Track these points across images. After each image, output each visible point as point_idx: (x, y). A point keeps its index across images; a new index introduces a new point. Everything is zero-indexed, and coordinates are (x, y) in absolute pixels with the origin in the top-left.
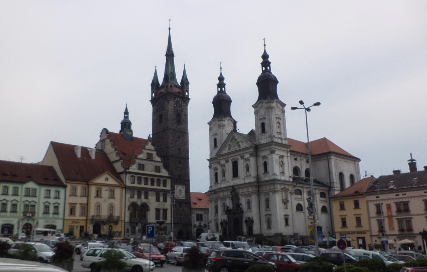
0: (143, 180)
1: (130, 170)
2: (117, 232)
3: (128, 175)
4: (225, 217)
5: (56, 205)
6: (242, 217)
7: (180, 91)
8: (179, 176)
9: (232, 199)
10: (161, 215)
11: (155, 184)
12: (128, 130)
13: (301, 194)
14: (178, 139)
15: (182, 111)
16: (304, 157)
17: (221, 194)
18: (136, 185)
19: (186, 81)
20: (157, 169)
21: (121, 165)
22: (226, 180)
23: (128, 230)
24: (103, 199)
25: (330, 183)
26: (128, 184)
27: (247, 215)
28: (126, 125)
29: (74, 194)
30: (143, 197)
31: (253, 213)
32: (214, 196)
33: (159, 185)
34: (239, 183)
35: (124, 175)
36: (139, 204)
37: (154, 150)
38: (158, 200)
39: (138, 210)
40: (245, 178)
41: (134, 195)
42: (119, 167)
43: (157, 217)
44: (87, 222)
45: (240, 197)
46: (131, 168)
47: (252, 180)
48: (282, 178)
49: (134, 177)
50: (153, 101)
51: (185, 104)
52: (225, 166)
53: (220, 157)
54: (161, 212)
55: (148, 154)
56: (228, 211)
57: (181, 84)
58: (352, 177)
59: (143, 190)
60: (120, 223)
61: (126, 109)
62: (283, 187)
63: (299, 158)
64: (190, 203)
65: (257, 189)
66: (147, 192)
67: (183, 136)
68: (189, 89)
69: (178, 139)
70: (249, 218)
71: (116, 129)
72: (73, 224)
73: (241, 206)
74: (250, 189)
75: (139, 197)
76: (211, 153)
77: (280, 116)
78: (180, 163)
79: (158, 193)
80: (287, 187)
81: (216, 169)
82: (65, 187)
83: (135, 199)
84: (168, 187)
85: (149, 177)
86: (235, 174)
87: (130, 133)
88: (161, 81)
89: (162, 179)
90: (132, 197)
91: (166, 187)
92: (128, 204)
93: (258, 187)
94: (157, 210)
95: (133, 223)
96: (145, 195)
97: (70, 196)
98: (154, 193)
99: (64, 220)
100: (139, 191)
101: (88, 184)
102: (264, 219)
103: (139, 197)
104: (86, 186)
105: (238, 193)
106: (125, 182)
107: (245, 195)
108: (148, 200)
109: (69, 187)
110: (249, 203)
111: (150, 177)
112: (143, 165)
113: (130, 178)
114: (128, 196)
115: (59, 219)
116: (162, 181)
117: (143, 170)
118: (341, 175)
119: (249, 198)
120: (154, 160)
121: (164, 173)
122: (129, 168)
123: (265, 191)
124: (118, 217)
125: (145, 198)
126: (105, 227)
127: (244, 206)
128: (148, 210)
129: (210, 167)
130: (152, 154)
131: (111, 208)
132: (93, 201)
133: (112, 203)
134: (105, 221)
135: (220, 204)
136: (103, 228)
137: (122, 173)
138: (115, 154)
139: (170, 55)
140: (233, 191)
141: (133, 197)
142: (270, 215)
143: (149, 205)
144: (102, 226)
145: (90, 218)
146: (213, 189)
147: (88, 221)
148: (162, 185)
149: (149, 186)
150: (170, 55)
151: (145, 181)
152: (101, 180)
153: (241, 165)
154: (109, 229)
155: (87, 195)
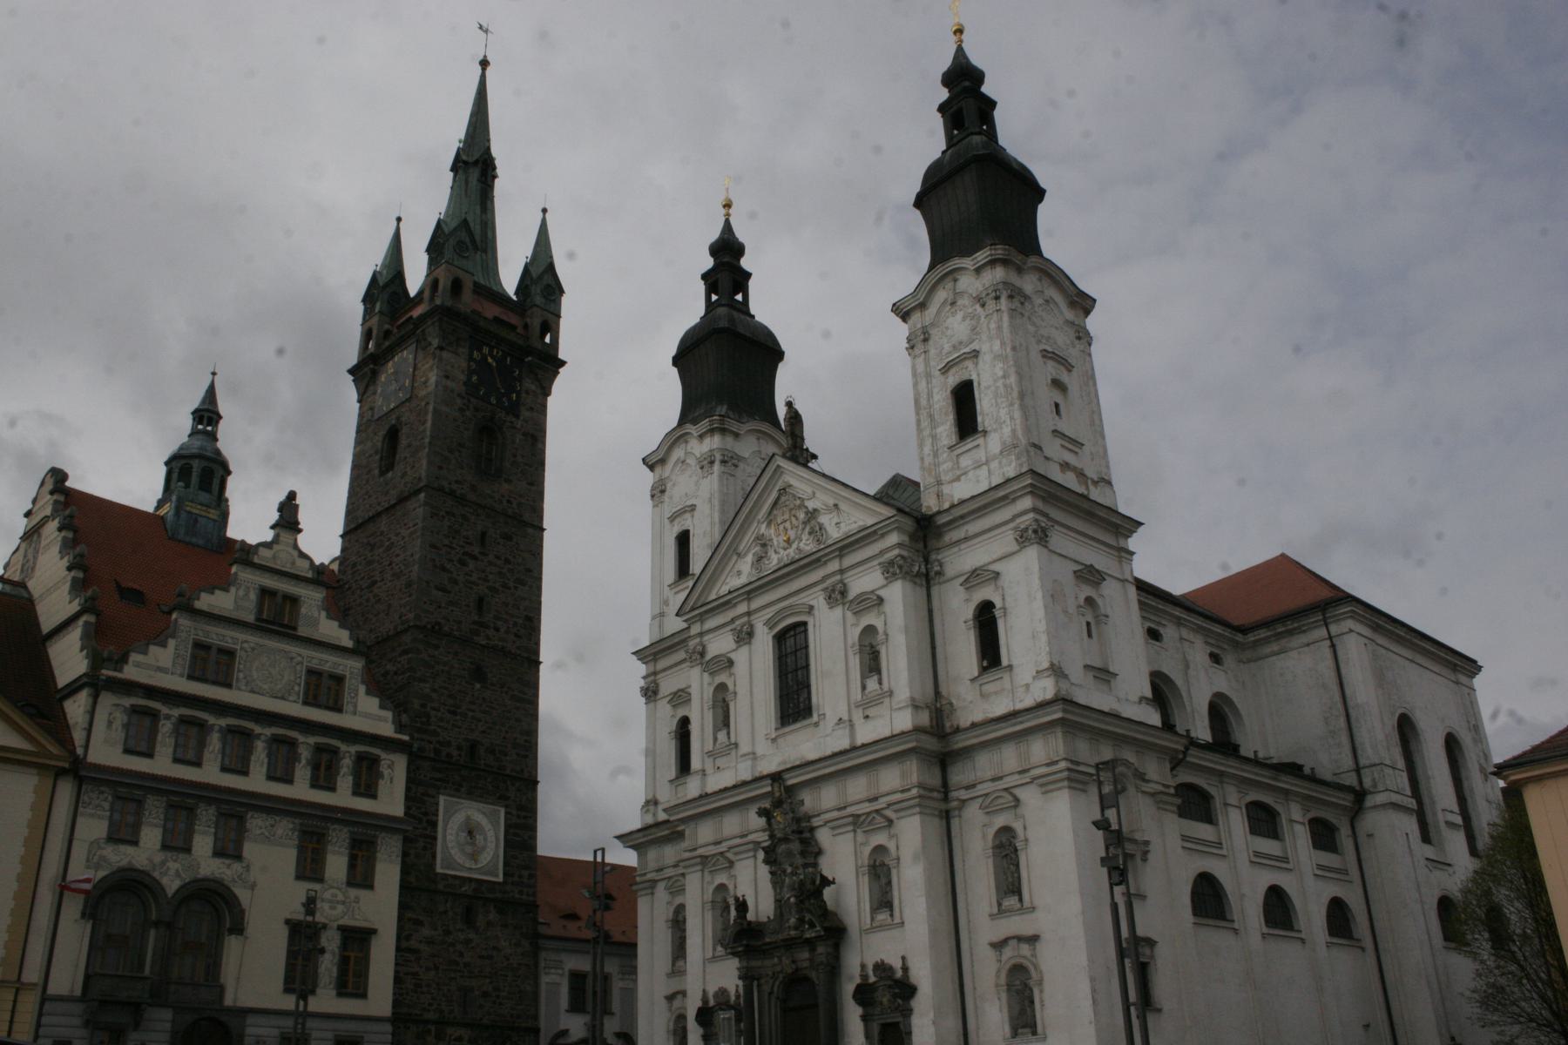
0: (214, 742)
1: (130, 672)
3: (107, 700)
4: (727, 976)
6: (834, 969)
7: (514, 319)
8: (473, 747)
10: (328, 966)
11: (302, 773)
12: (204, 497)
13: (1208, 817)
14: (476, 550)
15: (514, 409)
16: (1198, 630)
17: (704, 833)
18: (162, 764)
19: (547, 279)
20: (323, 688)
21: (79, 644)
22: (736, 745)
25: (1358, 770)
26: (105, 751)
27: (870, 949)
28: (199, 471)
30: (203, 844)
31: (906, 941)
32: (670, 853)
33: (324, 777)
34: (812, 756)
35: (83, 697)
36: (171, 885)
38: (310, 867)
39: (157, 924)
40: (857, 716)
41: (136, 827)
42: (68, 659)
43: (299, 978)
45: (823, 837)
46: (134, 657)
47: (904, 721)
48: (1099, 699)
49: (154, 715)
50: (365, 372)
51: (529, 384)
52: (731, 663)
53: (701, 618)
54: (331, 942)
55: (265, 593)
56: (743, 937)
57: (516, 293)
58: (1452, 745)
59: (210, 801)
61: (211, 393)
62: (1107, 754)
63: (1169, 632)
64: (532, 907)
65: (935, 781)
67: (507, 537)
68: (559, 316)
69: (476, 550)
70: (881, 967)
71: (132, 479)
73: (828, 893)
74: (890, 779)
75: (176, 843)
77: (1061, 339)
78: (479, 674)
79: (313, 830)
80: (1129, 755)
81: (680, 697)
83: (147, 850)
84: (391, 800)
86: (794, 702)
87: (213, 514)
88: (416, 276)
89: (349, 750)
90: (123, 834)
91: (374, 797)
93: (944, 760)
94: (303, 935)
100: (183, 801)
102: (986, 972)
103: (176, 843)
105: (809, 818)
106: (78, 736)
107: (857, 821)
108: (237, 866)
110: (880, 871)
112: (230, 654)
113: (120, 718)
114: (93, 828)
116: (347, 763)
118: (1406, 728)
119: (880, 839)
120: (303, 631)
121: (368, 713)
122: (124, 659)
123: (982, 789)
125: (219, 853)
127: (848, 891)
128: (238, 929)
130: (294, 600)
135: (696, 892)
137: (73, 688)
138: (67, 586)
139: (475, 167)
140: (778, 804)
141: (135, 843)
142: (1033, 939)
143: (242, 894)
148: (345, 782)
149: (256, 781)
150: (475, 167)
153: (831, 638)
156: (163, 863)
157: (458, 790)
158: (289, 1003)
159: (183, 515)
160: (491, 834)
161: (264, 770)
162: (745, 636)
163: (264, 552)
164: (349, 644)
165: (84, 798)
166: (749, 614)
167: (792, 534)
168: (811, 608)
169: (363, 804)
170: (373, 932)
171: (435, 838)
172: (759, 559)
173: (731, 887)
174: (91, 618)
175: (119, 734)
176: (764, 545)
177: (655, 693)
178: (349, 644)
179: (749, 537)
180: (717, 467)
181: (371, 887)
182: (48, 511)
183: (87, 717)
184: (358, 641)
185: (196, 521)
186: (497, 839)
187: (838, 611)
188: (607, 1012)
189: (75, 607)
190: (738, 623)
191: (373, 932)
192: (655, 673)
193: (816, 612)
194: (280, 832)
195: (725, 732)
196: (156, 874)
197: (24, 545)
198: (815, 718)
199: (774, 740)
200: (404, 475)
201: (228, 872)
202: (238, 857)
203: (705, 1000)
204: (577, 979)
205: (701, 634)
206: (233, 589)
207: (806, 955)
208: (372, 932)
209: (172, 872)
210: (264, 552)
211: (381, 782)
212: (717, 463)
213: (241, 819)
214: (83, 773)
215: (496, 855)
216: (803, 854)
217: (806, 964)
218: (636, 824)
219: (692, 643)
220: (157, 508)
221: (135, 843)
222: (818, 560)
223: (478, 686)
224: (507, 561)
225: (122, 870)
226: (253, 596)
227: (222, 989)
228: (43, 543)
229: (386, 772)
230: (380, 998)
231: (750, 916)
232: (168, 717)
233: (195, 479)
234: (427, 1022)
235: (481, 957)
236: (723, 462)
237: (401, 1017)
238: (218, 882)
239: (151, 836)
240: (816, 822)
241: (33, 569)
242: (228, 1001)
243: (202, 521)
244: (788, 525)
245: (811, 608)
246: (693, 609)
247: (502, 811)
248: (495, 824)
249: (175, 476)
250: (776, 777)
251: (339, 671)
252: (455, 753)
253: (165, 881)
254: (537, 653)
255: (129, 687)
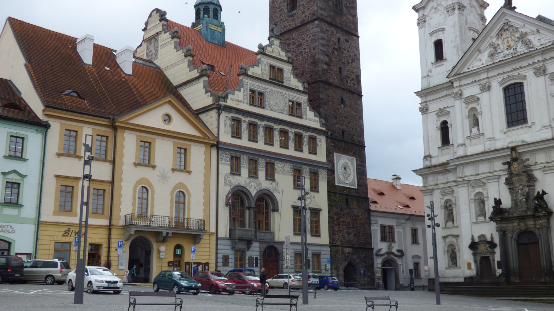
0: (261, 133)
1: (229, 103)
2: (198, 264)
3: (224, 115)
4: (489, 230)
5: (14, 178)
9: (508, 182)
12: (215, 21)
17: (469, 172)
18: (244, 142)
20: (295, 108)
23: (226, 258)
24: (156, 171)
26: (226, 138)
29: (69, 152)
30: (262, 174)
35: (214, 113)
36: (253, 192)
37: (288, 62)
38: (298, 185)
39: (249, 208)
42: (198, 96)
43: (299, 229)
44: (110, 234)
45: (537, 174)
46: (230, 96)
53: (460, 79)
55: (272, 67)
56: (499, 214)
60: (205, 237)
66: (271, 162)
67: (347, 41)
72: (67, 239)
73: (545, 197)
76: (426, 77)
79: (297, 167)
82: (45, 126)
83: (243, 178)
84: (321, 156)
85: (275, 126)
87: (220, 30)
89: (306, 134)
90: (235, 171)
91: (316, 154)
92: (225, 190)
94: (297, 211)
95: (239, 241)
96: (267, 170)
97: (59, 155)
98: (288, 167)
99: (39, 223)
100: (254, 157)
101: (115, 128)
103: (253, 174)
104: (108, 132)
105: (529, 166)
108: (274, 184)
109: (56, 126)
111: (278, 127)
112: (261, 94)
113: (229, 122)
114: (225, 169)
115: (23, 221)
117: (261, 106)
121: (311, 119)
122: (225, 98)
124: (203, 223)
126: (163, 248)
128: (276, 210)
129: (424, 110)
130: (281, 70)
131: (181, 198)
132: (130, 177)
133: (181, 184)
134: (164, 232)
136: (159, 252)
137: (206, 110)
141: (240, 175)
143: (278, 196)
144: (155, 246)
145: (122, 222)
146: (434, 162)
147: (113, 231)
148: (306, 148)
149: (276, 149)
151: (265, 135)
152: (152, 118)
154: (175, 255)
155: (110, 157)
156: (250, 183)
157: (340, 151)
158: (298, 239)
159: (209, 30)
160: (352, 169)
161: (263, 141)
162: (487, 88)
163: (269, 49)
164: (302, 89)
165: (220, 156)
166: (488, 78)
167: (512, 43)
168: (525, 76)
169: (312, 157)
170: (320, 210)
171: (334, 171)
172: (492, 55)
173: (485, 193)
174: (206, 79)
175: (229, 129)
176: (495, 48)
177: (427, 110)
178: (302, 89)
179: (486, 44)
180: (456, 10)
181: (318, 192)
182: (160, 29)
183: (216, 122)
184: (305, 88)
185: (214, 33)
186: (354, 171)
187: (542, 79)
188: (394, 241)
189: (195, 73)
190: (481, 82)
191: (320, 210)
192: (426, 102)
193: (528, 77)
194: (286, 169)
195: (476, 128)
196: (248, 188)
197: (145, 45)
198: (529, 123)
199: (505, 133)
200: (303, 13)
201: (271, 186)
202: (274, 180)
203: (473, 238)
204: (383, 227)
205: (460, 86)
206: (260, 65)
207: (532, 223)
208: (320, 210)
209: (253, 187)
210: (269, 49)
211: (318, 148)
212: (456, 10)
213: (273, 164)
214: (220, 146)
215: (354, 178)
216: (528, 181)
217: (533, 226)
218: (421, 166)
219: (455, 91)
220: (194, 25)
221: (240, 175)
222: (530, 55)
223: (343, 106)
224: (348, 52)
225: (236, 186)
226: (267, 68)
227: (273, 234)
228: (160, 44)
229: (319, 143)
230: (325, 238)
231: (502, 206)
232: (244, 122)
233: (211, 14)
234: (338, 246)
235: (353, 219)
236: (459, 9)
237: (332, 244)
238: (269, 191)
239: (244, 171)
240: (533, 168)
241: (156, 55)
242: (276, 239)
243: (216, 33)
244: (509, 39)
245: (525, 77)
246: (455, 75)
247: (355, 159)
248: (353, 164)
249: (202, 12)
250: (513, 149)
251: (299, 101)
252: (338, 135)
253: (251, 190)
254: (361, 92)
255: (230, 109)
